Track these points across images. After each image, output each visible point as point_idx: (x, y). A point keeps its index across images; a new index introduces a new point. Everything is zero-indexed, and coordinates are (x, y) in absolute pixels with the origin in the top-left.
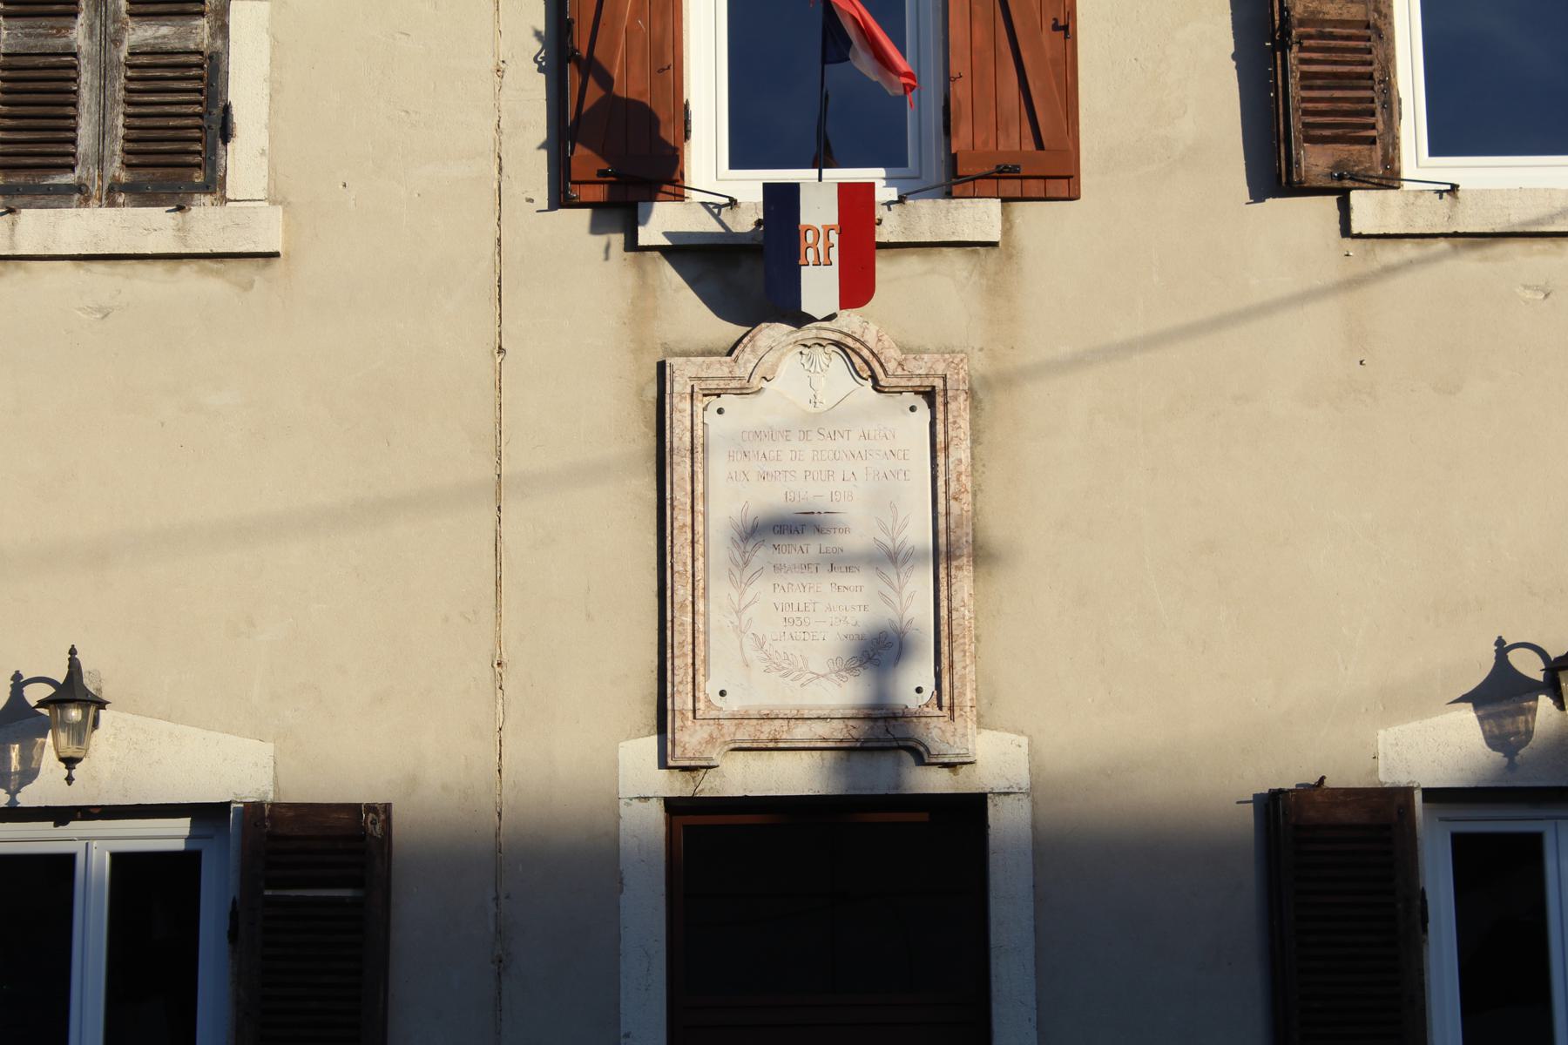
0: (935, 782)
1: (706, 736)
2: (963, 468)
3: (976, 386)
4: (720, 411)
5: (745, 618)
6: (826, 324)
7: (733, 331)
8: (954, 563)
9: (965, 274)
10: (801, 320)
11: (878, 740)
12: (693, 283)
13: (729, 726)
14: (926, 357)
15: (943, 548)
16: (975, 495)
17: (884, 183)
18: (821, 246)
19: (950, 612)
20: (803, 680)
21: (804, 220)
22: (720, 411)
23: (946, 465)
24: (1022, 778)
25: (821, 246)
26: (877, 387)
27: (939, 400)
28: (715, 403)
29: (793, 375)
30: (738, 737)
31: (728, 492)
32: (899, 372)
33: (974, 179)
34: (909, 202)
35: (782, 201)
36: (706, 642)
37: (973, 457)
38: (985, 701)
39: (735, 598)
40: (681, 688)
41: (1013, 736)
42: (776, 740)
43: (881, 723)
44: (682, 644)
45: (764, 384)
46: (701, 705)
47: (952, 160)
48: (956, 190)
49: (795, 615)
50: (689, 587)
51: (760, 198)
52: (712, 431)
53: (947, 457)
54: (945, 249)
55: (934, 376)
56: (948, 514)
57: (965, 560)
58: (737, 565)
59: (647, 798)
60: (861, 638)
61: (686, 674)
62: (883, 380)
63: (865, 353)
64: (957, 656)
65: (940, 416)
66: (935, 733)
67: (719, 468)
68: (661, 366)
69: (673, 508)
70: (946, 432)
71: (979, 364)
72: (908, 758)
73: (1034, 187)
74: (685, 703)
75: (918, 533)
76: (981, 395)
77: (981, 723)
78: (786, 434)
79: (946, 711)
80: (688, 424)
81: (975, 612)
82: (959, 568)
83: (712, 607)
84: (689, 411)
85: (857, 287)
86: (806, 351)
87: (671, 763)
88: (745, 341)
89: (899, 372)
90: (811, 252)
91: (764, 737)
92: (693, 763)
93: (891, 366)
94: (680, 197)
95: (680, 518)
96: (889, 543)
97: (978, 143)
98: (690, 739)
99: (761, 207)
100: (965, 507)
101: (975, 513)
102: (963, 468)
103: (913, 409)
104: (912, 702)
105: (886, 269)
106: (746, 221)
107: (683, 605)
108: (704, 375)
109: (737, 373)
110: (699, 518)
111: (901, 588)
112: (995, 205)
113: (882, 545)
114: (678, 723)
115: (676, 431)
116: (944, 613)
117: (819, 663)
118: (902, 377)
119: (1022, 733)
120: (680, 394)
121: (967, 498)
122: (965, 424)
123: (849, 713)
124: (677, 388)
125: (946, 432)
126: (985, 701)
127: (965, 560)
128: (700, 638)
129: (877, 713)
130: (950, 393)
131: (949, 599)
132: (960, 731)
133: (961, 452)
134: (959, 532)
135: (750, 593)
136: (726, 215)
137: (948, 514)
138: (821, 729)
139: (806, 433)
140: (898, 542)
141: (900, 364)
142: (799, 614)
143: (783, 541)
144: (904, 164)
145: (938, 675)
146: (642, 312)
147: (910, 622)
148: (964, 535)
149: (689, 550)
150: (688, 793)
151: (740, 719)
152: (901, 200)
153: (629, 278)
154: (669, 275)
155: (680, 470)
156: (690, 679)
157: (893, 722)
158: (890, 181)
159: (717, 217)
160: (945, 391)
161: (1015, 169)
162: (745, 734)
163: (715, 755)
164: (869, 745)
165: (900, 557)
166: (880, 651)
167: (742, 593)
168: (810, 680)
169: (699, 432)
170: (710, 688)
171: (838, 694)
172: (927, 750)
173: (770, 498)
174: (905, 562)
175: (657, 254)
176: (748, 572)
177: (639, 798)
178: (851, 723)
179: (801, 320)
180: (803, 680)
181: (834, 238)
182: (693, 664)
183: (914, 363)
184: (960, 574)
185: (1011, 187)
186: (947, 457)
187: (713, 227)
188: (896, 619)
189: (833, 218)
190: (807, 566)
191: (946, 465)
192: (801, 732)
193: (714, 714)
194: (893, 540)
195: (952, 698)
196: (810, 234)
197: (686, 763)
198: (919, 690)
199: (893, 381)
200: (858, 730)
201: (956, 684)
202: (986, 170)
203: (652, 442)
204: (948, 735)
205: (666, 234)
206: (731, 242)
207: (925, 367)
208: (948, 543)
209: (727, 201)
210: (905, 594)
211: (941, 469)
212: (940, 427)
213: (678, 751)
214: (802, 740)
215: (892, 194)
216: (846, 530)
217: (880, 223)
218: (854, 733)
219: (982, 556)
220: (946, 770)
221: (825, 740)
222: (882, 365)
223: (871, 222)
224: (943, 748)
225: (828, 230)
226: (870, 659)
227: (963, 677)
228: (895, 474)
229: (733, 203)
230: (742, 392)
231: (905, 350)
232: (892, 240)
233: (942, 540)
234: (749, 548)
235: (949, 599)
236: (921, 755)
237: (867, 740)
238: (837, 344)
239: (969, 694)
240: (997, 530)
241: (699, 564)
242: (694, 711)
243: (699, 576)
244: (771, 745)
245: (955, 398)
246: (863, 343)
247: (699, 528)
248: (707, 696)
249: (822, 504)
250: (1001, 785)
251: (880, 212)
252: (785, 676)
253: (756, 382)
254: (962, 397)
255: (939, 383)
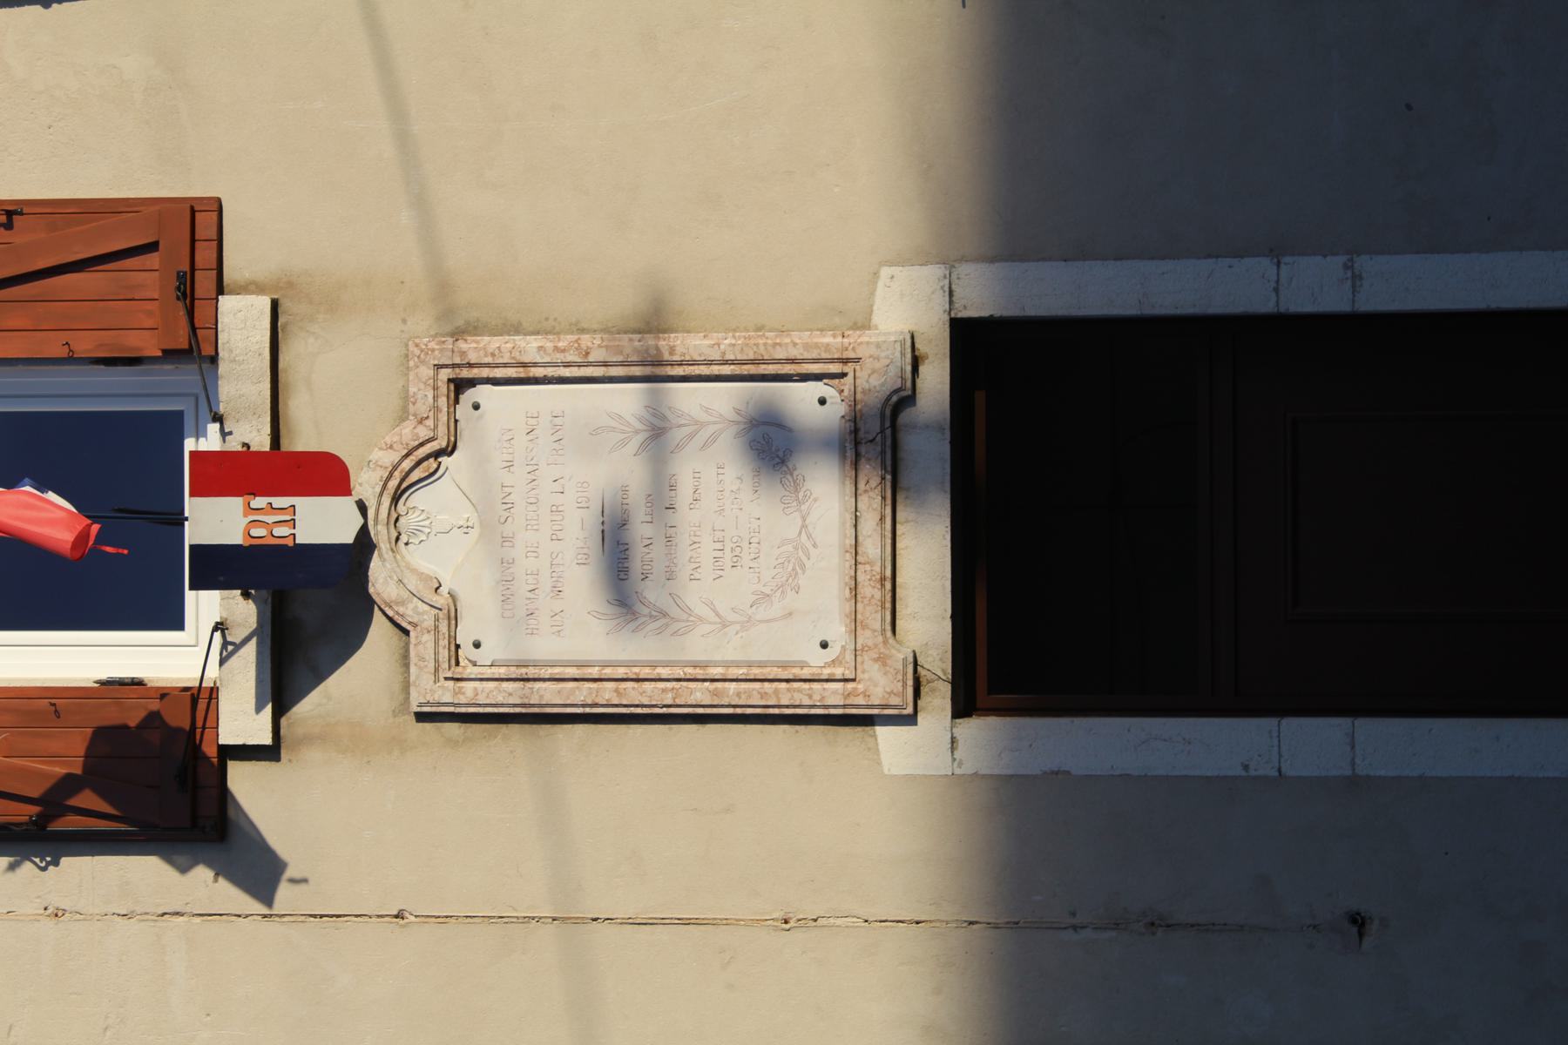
0: (935, 381)
1: (876, 666)
2: (549, 345)
3: (449, 328)
4: (477, 645)
5: (732, 617)
6: (371, 513)
7: (379, 628)
8: (666, 357)
9: (311, 340)
10: (364, 545)
11: (883, 452)
12: (320, 676)
13: (865, 637)
14: (412, 390)
15: (647, 371)
16: (583, 331)
17: (202, 440)
18: (270, 519)
19: (726, 362)
20: (809, 545)
21: (236, 538)
22: (477, 645)
23: (545, 365)
24: (929, 277)
25: (270, 519)
26: (449, 451)
27: (465, 373)
28: (467, 651)
29: (433, 555)
30: (877, 626)
31: (576, 636)
32: (430, 423)
33: (194, 329)
34: (222, 409)
35: (218, 567)
36: (761, 665)
37: (538, 333)
38: (837, 320)
39: (707, 628)
40: (817, 697)
41: (880, 284)
42: (883, 579)
43: (863, 449)
44: (763, 695)
45: (444, 590)
46: (838, 672)
47: (171, 355)
48: (207, 350)
49: (728, 554)
50: (692, 685)
51: (215, 595)
52: (499, 655)
53: (535, 365)
54: (281, 365)
55: (435, 379)
56: (605, 364)
57: (662, 343)
58: (667, 625)
59: (953, 740)
60: (757, 472)
61: (799, 691)
62: (441, 443)
63: (407, 464)
64: (780, 354)
65: (485, 372)
66: (875, 382)
67: (545, 647)
68: (421, 717)
69: (596, 705)
70: (505, 365)
71: (422, 325)
72: (905, 417)
73: (205, 255)
74: (835, 692)
75: (627, 400)
76: (460, 323)
77: (865, 325)
78: (506, 563)
79: (848, 369)
80: (492, 685)
81: (727, 330)
82: (672, 351)
83: (718, 657)
84: (477, 684)
85: (325, 475)
86: (404, 538)
87: (910, 710)
88: (390, 613)
89: (430, 423)
90: (278, 531)
91: (878, 595)
92: (910, 682)
93: (424, 433)
94: (213, 692)
95: (606, 695)
96: (640, 437)
97: (149, 323)
98: (880, 686)
99: (226, 593)
100: (598, 342)
101: (605, 330)
102: (549, 345)
103: (476, 407)
104: (837, 410)
105: (304, 438)
106: (243, 611)
107: (715, 693)
108: (432, 665)
109: (429, 623)
110: (608, 672)
111: (697, 422)
112: (226, 302)
113: (644, 446)
114: (861, 701)
115: (500, 699)
116: (727, 370)
117: (788, 525)
118: (436, 420)
119: (876, 274)
120: (456, 694)
121: (586, 340)
122: (494, 343)
123: (850, 488)
124: (447, 698)
125: (505, 365)
126: (837, 320)
127: (662, 343)
128: (756, 672)
129: (850, 454)
130: (457, 360)
131: (710, 363)
132: (873, 351)
133: (530, 347)
134: (628, 350)
135: (701, 610)
136: (236, 636)
137: (605, 364)
138: (869, 524)
139: (505, 539)
140: (639, 426)
141: (421, 422)
142: (727, 550)
143: (636, 566)
144: (179, 415)
145: (804, 378)
146: (351, 740)
147: (738, 412)
148: (630, 345)
149: (647, 685)
150: (946, 689)
151: (855, 624)
152: (218, 418)
153: (313, 755)
154: (308, 708)
155: (549, 696)
156: (806, 686)
157: (861, 434)
158: (199, 433)
159: (238, 647)
160: (454, 366)
161: (181, 277)
162: (874, 618)
163: (900, 654)
164: (889, 463)
165: (657, 422)
166: (771, 446)
167: (700, 619)
168: (809, 537)
169: (502, 672)
170: (818, 661)
171: (827, 498)
172: (896, 391)
173: (582, 583)
174: (664, 418)
175: (284, 721)
176: (674, 612)
177: (953, 749)
178: (861, 486)
179: (364, 545)
180: (809, 545)
181: (259, 502)
182: (787, 681)
183: (419, 404)
184: (679, 350)
185: (204, 282)
186: (535, 365)
187: (250, 652)
188: (734, 429)
189: (236, 503)
190: (669, 539)
191: (545, 365)
192: (873, 547)
193: (849, 657)
194: (637, 432)
195: (832, 361)
196: (254, 532)
197: (910, 691)
198: (822, 401)
199: (442, 430)
200: (871, 475)
201: (814, 356)
202: (182, 313)
203: (515, 728)
204: (878, 365)
205: (259, 709)
206: (268, 629)
207: (425, 391)
208: (642, 363)
209: (218, 635)
210: (703, 417)
211: (550, 372)
212: (499, 373)
213: (895, 701)
214: (883, 547)
215: (213, 428)
216: (625, 491)
217: (246, 445)
218: (875, 481)
219: (654, 321)
220: (921, 369)
221: (882, 519)
222: (422, 445)
223: (246, 456)
224: (893, 371)
225: (249, 509)
226: (783, 462)
227: (807, 346)
228: (556, 429)
229: (219, 627)
230: (454, 618)
231: (403, 418)
232: (267, 429)
233: (637, 371)
234: (645, 611)
235: (710, 363)
236: (901, 401)
237: (883, 466)
238: (396, 499)
239: (828, 339)
240: (623, 302)
241: (664, 672)
242: (846, 680)
243: (679, 673)
244: (888, 585)
245: (463, 354)
246: (395, 468)
247: (620, 672)
248: (827, 665)
249: (592, 518)
250: (941, 301)
251: (234, 445)
252: (803, 567)
253: (441, 600)
254: (462, 345)
255: (445, 374)
